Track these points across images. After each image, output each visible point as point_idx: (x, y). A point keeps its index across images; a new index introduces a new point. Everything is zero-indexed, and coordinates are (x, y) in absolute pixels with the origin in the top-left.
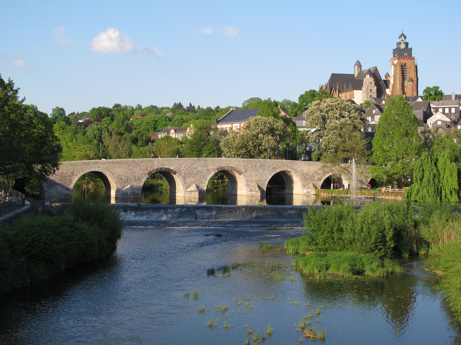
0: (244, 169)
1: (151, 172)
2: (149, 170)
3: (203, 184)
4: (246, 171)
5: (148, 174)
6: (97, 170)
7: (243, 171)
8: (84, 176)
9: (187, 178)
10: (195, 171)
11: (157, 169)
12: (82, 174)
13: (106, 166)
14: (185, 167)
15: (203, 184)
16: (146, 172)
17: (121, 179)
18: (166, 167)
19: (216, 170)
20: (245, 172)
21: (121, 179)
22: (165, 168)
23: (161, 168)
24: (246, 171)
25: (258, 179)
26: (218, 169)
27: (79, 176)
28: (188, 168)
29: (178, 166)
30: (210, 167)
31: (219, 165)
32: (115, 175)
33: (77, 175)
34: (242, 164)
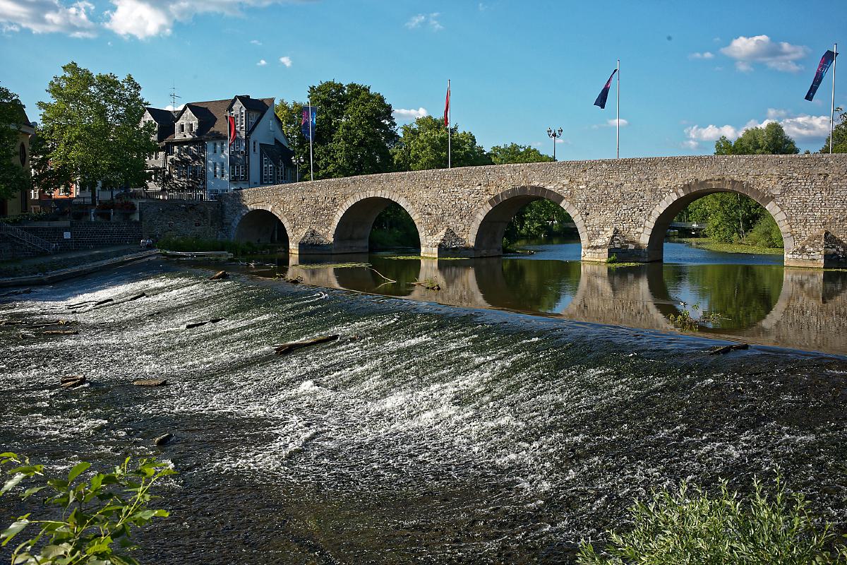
0: (779, 187)
1: (496, 198)
3: (640, 230)
4: (786, 190)
5: (490, 201)
6: (379, 195)
7: (778, 192)
9: (593, 214)
11: (513, 190)
15: (640, 230)
17: (429, 214)
18: (536, 184)
19: (680, 191)
21: (429, 214)
24: (786, 190)
25: (833, 215)
28: (597, 186)
30: (662, 183)
32: (416, 206)
33: (341, 205)
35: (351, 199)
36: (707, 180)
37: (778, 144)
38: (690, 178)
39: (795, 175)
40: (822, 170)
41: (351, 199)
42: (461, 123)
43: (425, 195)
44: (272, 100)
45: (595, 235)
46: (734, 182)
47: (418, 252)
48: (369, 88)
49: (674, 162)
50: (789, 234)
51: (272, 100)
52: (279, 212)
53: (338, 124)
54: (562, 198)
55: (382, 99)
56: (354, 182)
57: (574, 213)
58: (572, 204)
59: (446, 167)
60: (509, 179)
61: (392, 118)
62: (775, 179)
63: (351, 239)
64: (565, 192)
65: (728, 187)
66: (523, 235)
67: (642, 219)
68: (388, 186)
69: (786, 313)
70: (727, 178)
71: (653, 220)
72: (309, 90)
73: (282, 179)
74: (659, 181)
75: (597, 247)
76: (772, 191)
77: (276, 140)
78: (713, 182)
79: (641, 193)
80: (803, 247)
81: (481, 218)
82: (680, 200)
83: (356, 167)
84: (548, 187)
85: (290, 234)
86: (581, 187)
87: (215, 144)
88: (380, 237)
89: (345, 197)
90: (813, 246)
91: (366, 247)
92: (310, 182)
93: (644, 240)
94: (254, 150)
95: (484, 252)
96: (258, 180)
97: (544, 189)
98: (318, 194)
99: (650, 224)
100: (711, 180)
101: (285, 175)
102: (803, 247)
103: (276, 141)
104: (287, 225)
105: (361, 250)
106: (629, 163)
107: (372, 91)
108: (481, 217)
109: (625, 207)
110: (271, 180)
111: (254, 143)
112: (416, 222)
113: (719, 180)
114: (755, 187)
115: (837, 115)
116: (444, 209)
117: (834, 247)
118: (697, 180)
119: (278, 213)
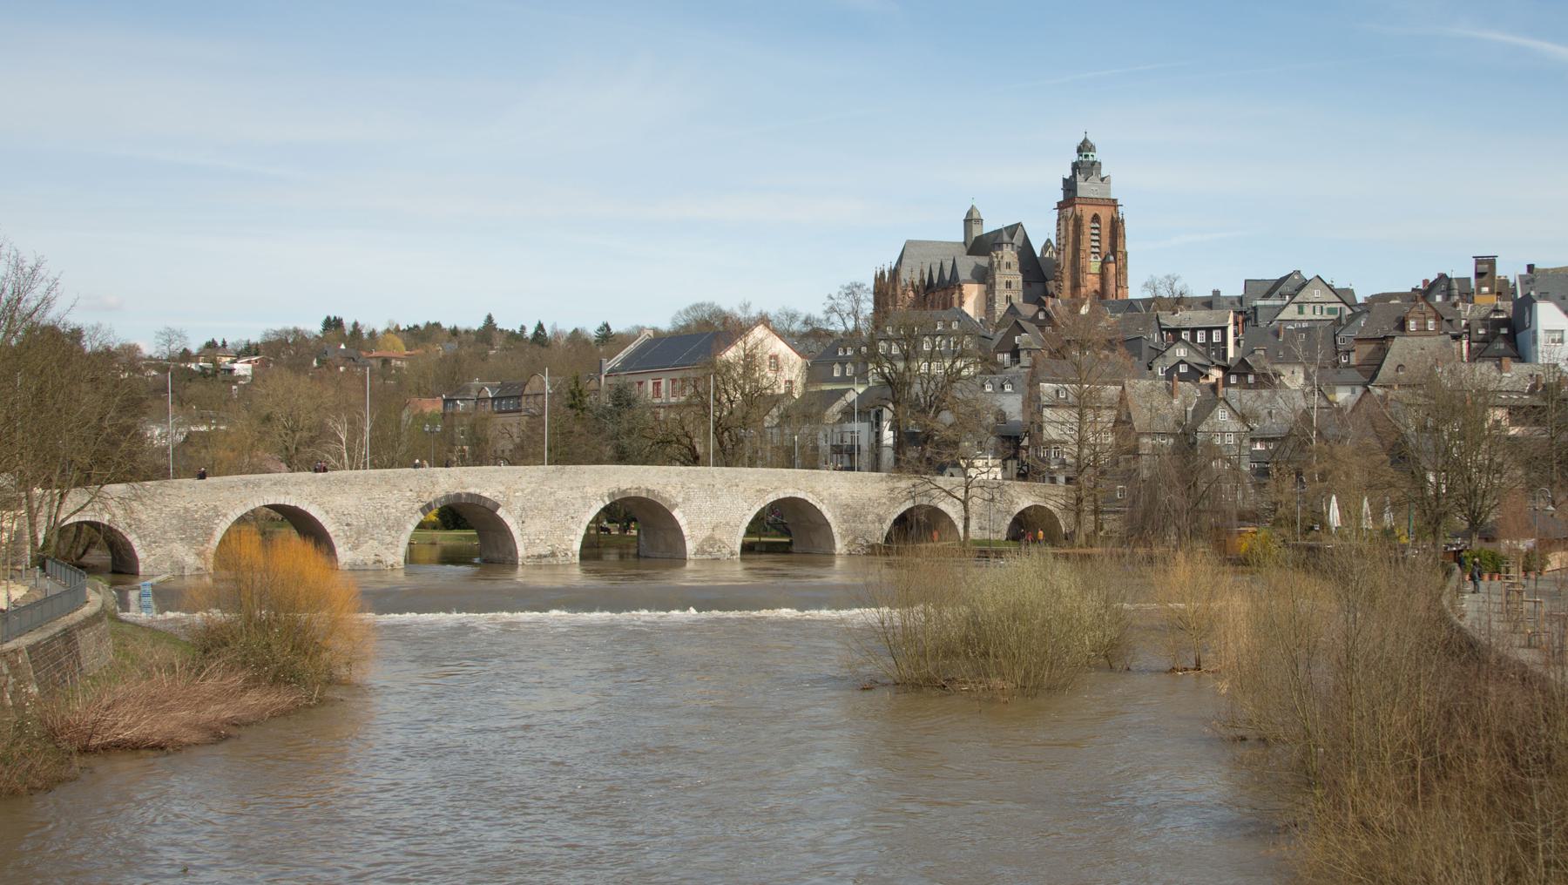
2: (427, 498)
4: (687, 499)
8: (242, 520)
9: (528, 521)
10: (551, 502)
11: (447, 497)
12: (240, 512)
13: (307, 490)
16: (418, 506)
18: (472, 490)
22: (469, 495)
23: (459, 495)
24: (687, 499)
26: (612, 495)
27: (233, 517)
28: (532, 493)
29: (502, 489)
30: (590, 491)
33: (225, 515)
34: (675, 479)
54: (498, 506)
56: (246, 485)
64: (500, 499)
74: (588, 489)
75: (540, 556)
97: (480, 497)
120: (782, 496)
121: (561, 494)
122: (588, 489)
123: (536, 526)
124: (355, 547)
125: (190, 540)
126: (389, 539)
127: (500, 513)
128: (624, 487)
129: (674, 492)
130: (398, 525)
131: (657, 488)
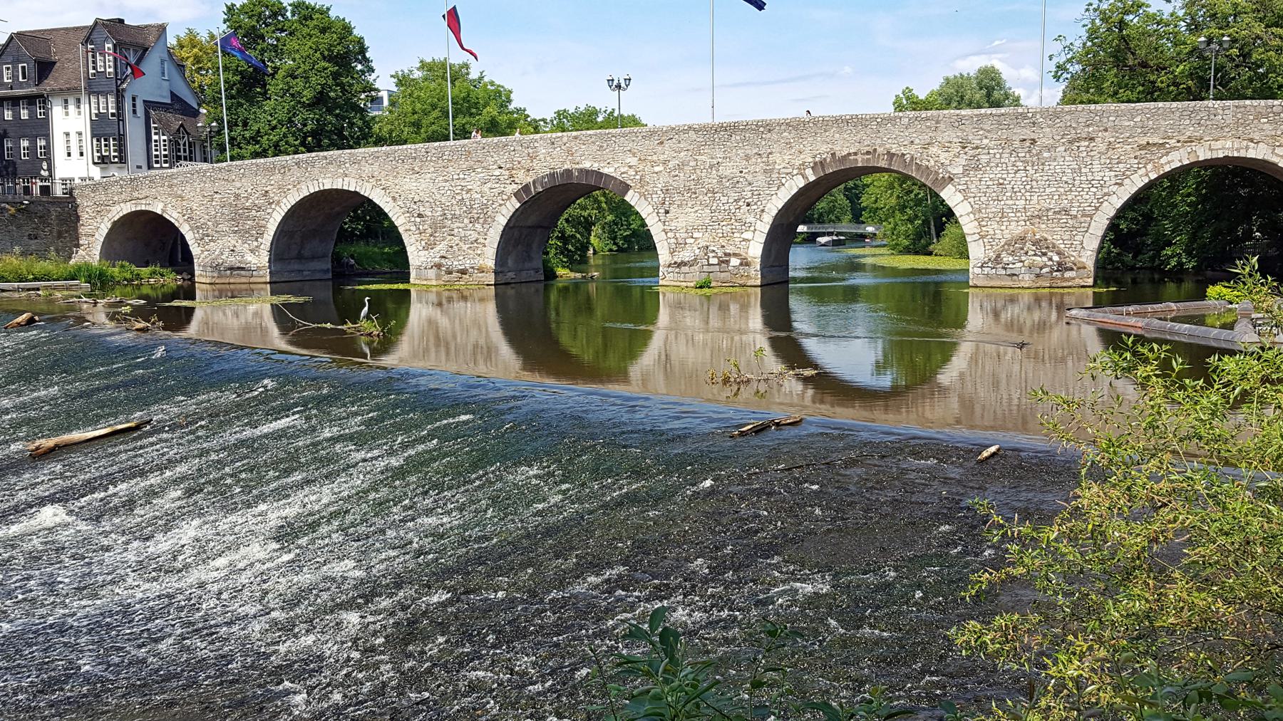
0: (962, 160)
1: (526, 188)
2: (524, 178)
3: (748, 235)
4: (973, 167)
5: (516, 195)
6: (339, 184)
7: (960, 170)
11: (552, 175)
13: (367, 169)
14: (665, 162)
15: (748, 235)
17: (420, 216)
18: (587, 165)
19: (809, 172)
20: (966, 172)
21: (420, 216)
22: (581, 171)
23: (568, 172)
24: (973, 167)
28: (680, 167)
29: (634, 161)
31: (824, 148)
33: (279, 202)
35: (294, 191)
36: (849, 154)
37: (988, 91)
38: (823, 150)
39: (985, 141)
40: (1028, 133)
41: (294, 191)
42: (491, 67)
43: (412, 186)
44: (162, 29)
45: (680, 245)
46: (891, 155)
47: (405, 278)
48: (328, 9)
49: (796, 126)
50: (977, 237)
51: (162, 29)
52: (175, 215)
53: (276, 69)
55: (347, 29)
57: (644, 209)
58: (643, 195)
59: (447, 138)
60: (548, 158)
61: (367, 60)
62: (956, 149)
63: (300, 257)
64: (629, 176)
65: (883, 164)
66: (572, 249)
67: (751, 219)
68: (352, 170)
69: (974, 360)
70: (880, 150)
71: (768, 219)
72: (225, 9)
73: (185, 159)
74: (776, 157)
76: (949, 169)
77: (173, 95)
78: (859, 158)
79: (750, 178)
80: (998, 256)
81: (503, 221)
82: (809, 187)
83: (317, 140)
84: (605, 171)
85: (195, 250)
86: (657, 169)
87: (66, 101)
88: (342, 256)
89: (283, 190)
90: (1013, 253)
91: (327, 271)
92: (224, 164)
93: (755, 250)
94: (134, 112)
95: (511, 275)
96: (145, 166)
97: (599, 175)
98: (238, 185)
99: (764, 226)
100: (855, 154)
101: (191, 152)
102: (998, 256)
103: (173, 95)
104: (189, 237)
105: (318, 276)
106: (731, 129)
107: (333, 14)
108: (502, 221)
109: (724, 199)
110: (166, 162)
111: (134, 99)
112: (401, 230)
113: (868, 153)
114: (925, 163)
115: (1058, 46)
116: (448, 210)
117: (1044, 254)
118: (833, 155)
119: (173, 216)
120: (1203, 154)
121: (728, 170)
122: (776, 157)
123: (683, 218)
124: (429, 246)
125: (243, 234)
126: (474, 236)
127: (631, 198)
128: (842, 151)
129: (943, 157)
130: (485, 217)
131: (909, 151)
